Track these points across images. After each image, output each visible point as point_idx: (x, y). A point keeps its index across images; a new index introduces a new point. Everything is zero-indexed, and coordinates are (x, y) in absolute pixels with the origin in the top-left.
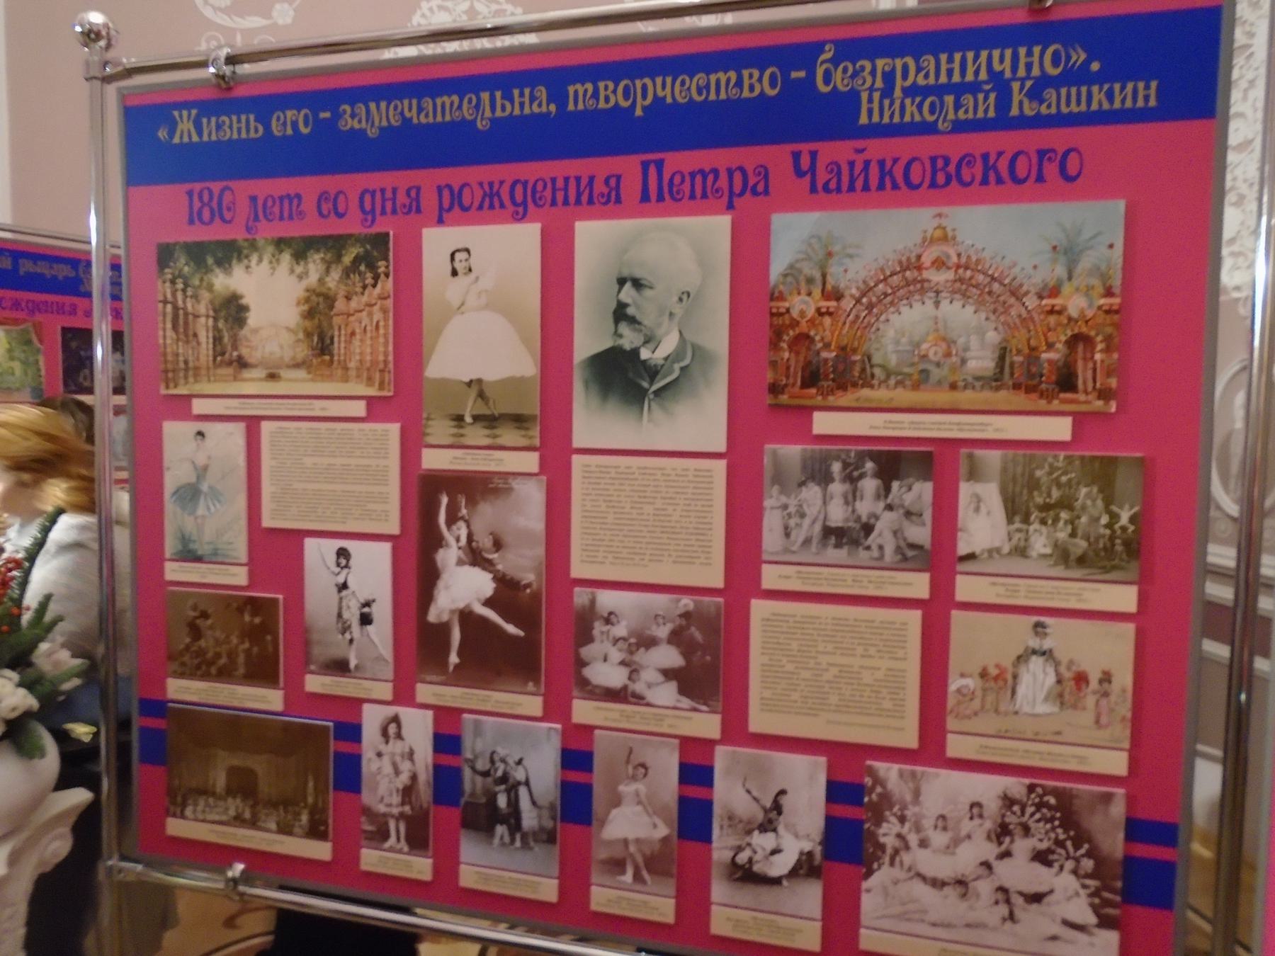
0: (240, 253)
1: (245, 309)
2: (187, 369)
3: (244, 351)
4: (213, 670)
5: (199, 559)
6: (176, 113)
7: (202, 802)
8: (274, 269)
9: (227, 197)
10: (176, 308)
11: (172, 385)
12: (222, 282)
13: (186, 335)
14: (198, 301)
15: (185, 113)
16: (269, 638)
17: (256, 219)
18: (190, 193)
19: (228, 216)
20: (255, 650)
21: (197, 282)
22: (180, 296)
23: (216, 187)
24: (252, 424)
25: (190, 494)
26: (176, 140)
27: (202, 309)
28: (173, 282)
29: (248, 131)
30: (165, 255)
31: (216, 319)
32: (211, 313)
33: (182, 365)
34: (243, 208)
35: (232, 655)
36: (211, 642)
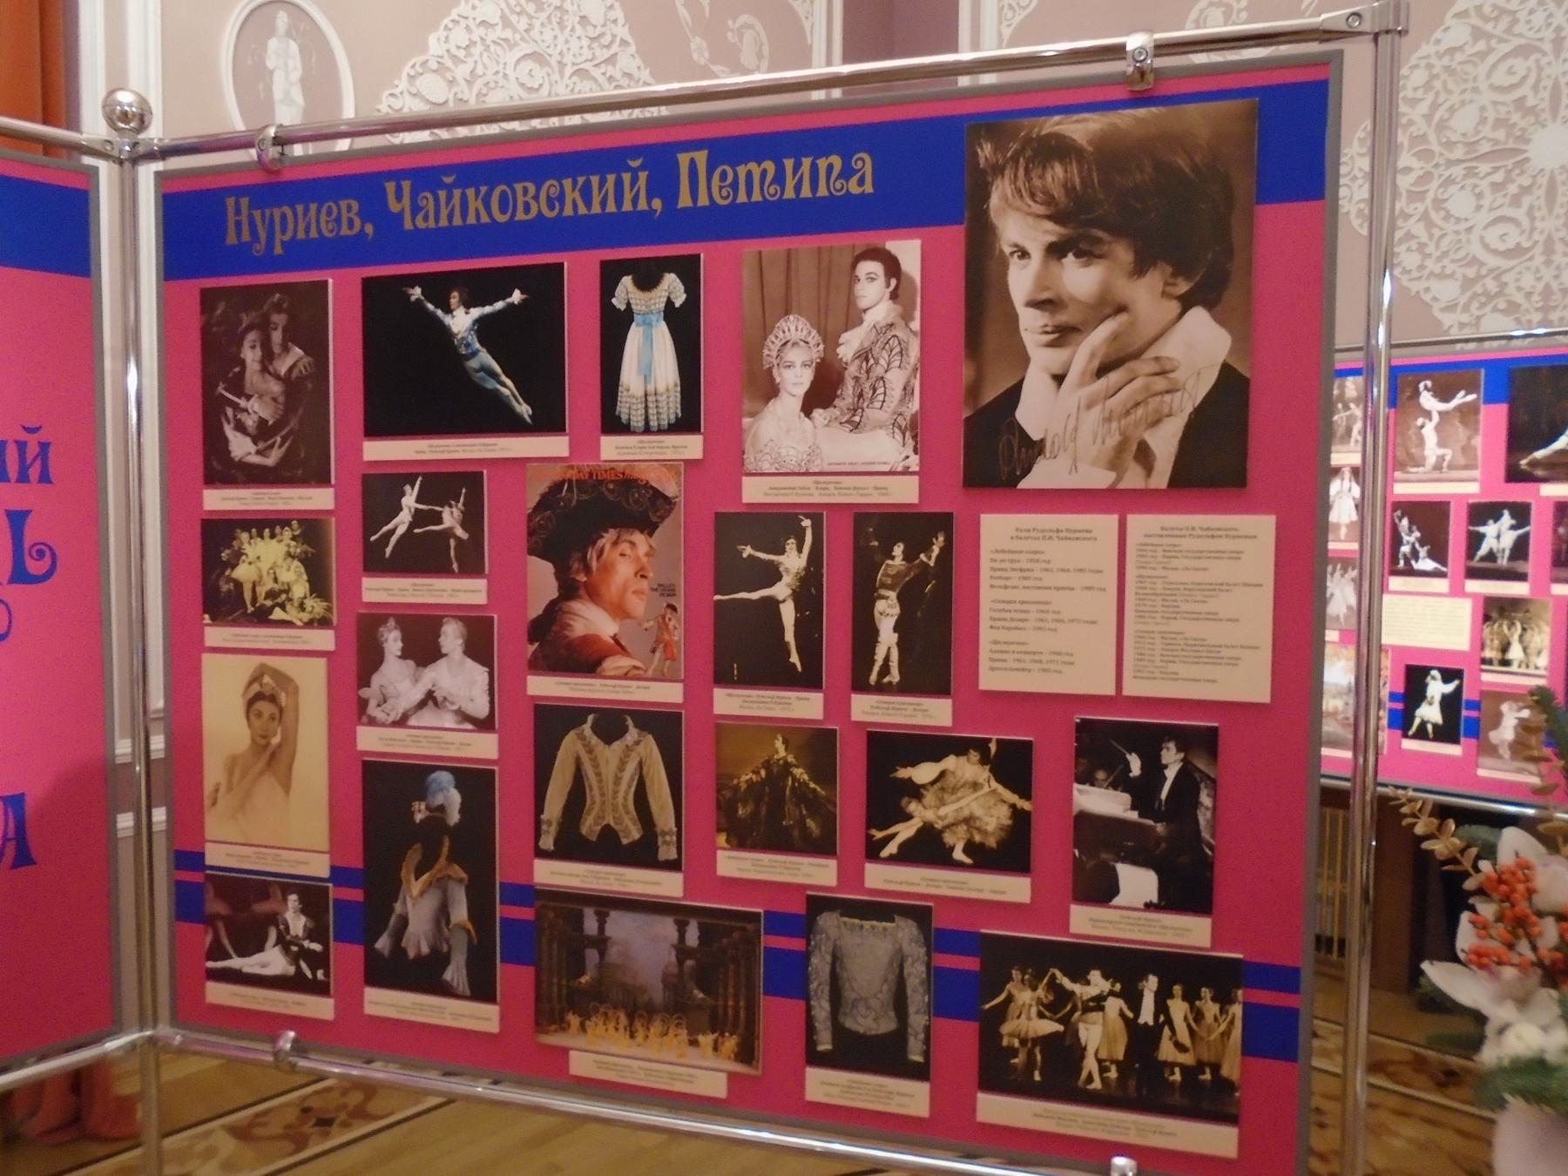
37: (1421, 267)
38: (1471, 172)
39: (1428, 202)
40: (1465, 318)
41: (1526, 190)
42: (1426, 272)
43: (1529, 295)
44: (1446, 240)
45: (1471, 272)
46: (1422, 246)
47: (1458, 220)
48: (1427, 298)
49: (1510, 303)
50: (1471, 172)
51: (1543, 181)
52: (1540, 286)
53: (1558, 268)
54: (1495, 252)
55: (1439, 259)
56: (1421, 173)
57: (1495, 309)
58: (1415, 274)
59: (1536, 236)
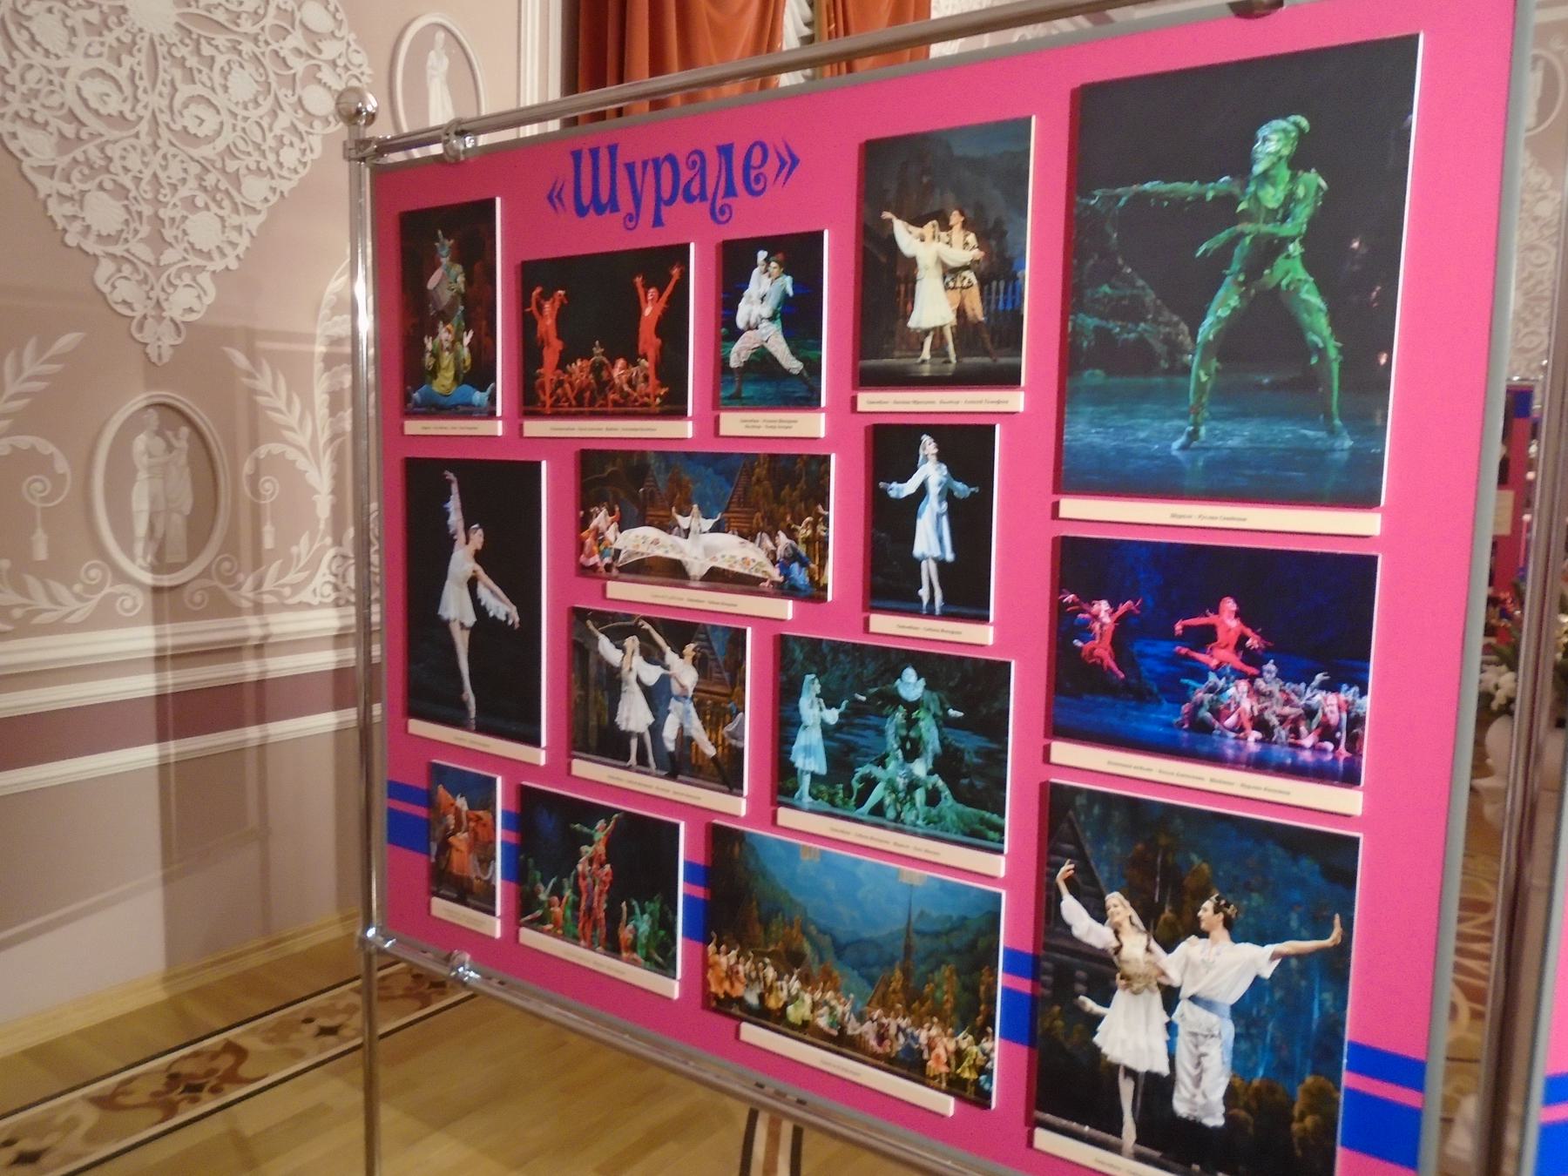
40: (66, 189)
44: (32, 76)
45: (69, 130)
47: (47, 53)
48: (13, 146)
51: (144, 44)
53: (165, 157)
54: (97, 113)
57: (101, 187)
59: (139, 107)
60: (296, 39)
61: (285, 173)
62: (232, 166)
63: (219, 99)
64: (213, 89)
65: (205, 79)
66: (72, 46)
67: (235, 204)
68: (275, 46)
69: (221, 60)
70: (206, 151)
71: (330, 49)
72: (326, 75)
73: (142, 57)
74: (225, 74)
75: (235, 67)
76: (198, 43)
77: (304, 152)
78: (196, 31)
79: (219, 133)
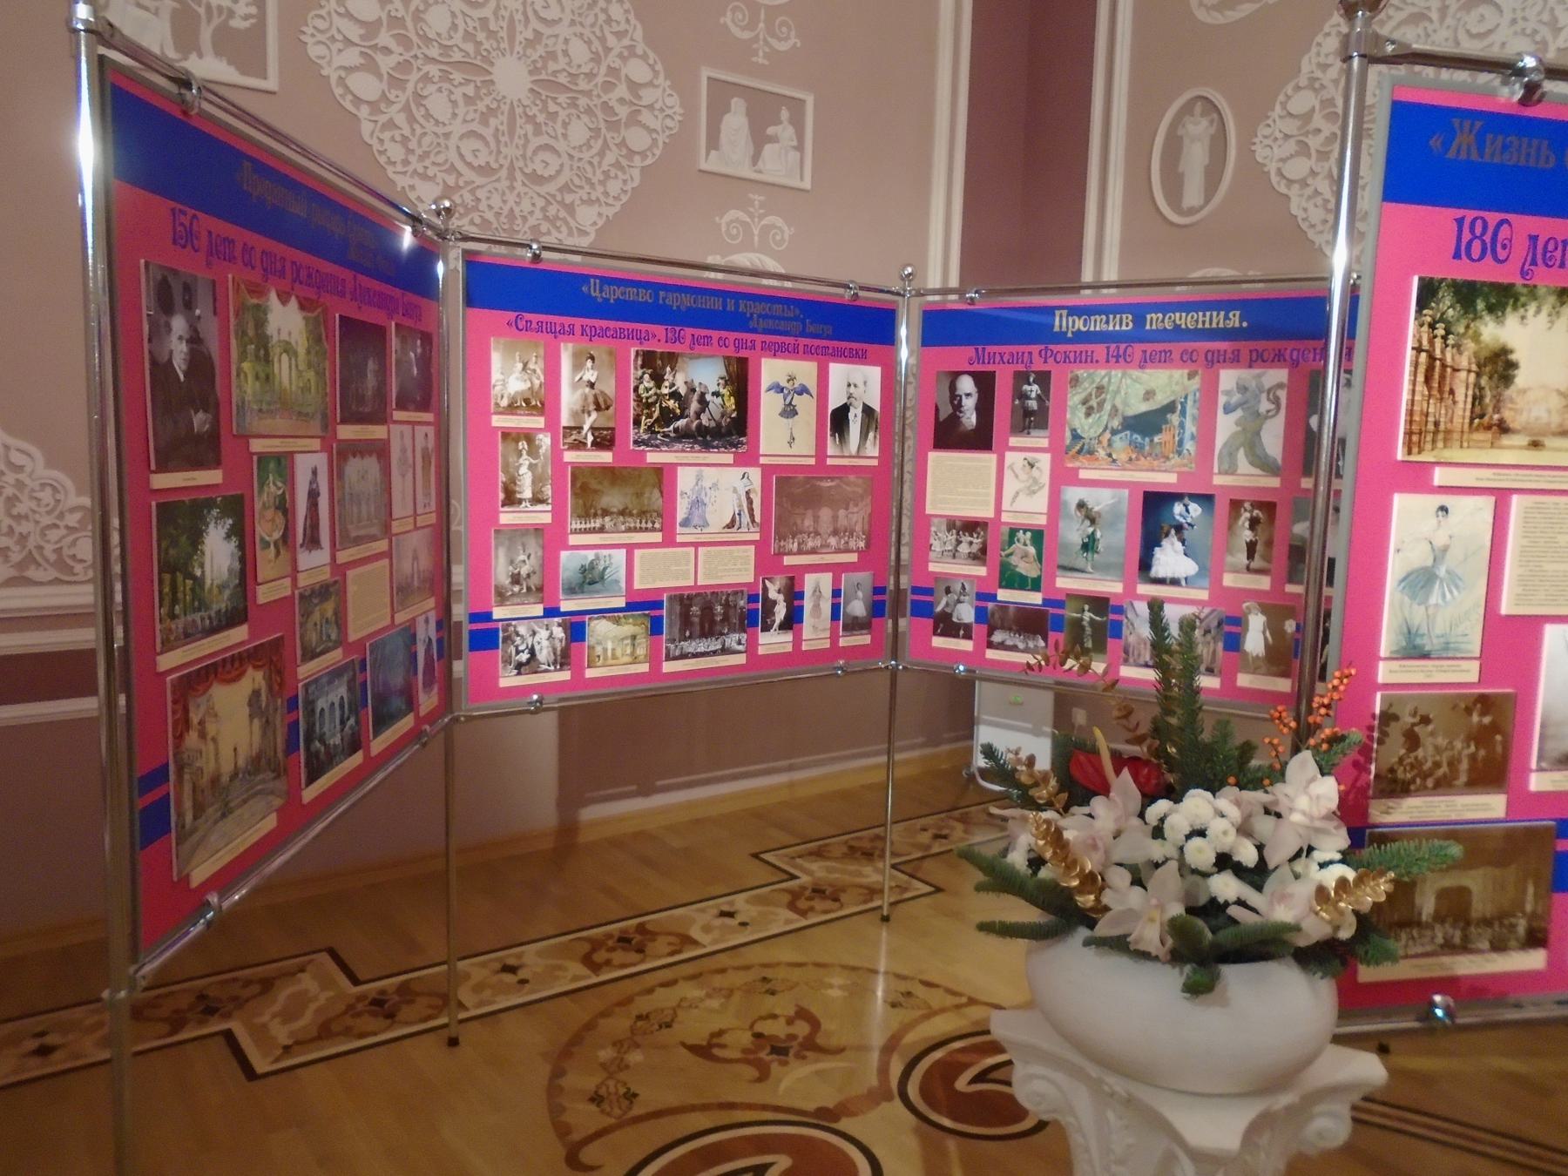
0: (1516, 300)
1: (1513, 365)
2: (1436, 432)
3: (1507, 414)
4: (1430, 783)
5: (1425, 656)
6: (1456, 122)
7: (1404, 936)
8: (1552, 322)
9: (1504, 232)
10: (1432, 358)
11: (1415, 450)
12: (1492, 331)
13: (1441, 391)
14: (1460, 353)
15: (1467, 124)
16: (1498, 738)
17: (1534, 263)
18: (1460, 222)
19: (1502, 254)
20: (1482, 753)
21: (1461, 330)
22: (1438, 343)
23: (1493, 218)
24: (1502, 497)
25: (1421, 581)
26: (1451, 154)
27: (1464, 362)
28: (1432, 326)
29: (1538, 159)
30: (1428, 292)
31: (1478, 375)
32: (1474, 367)
33: (1431, 427)
34: (1520, 249)
35: (1452, 764)
36: (1431, 750)
37: (406, 162)
38: (446, 76)
39: (409, 91)
41: (491, 112)
42: (410, 169)
43: (498, 214)
44: (427, 140)
45: (451, 180)
46: (405, 139)
47: (437, 122)
49: (484, 220)
50: (446, 76)
51: (506, 108)
52: (505, 212)
53: (519, 195)
54: (469, 164)
55: (421, 158)
56: (401, 59)
58: (399, 168)
60: (622, 91)
61: (610, 201)
62: (568, 198)
63: (561, 146)
64: (556, 138)
65: (550, 131)
66: (455, 115)
67: (570, 229)
68: (605, 98)
69: (563, 115)
70: (551, 188)
71: (648, 96)
72: (646, 117)
73: (505, 118)
74: (565, 125)
75: (574, 118)
76: (545, 103)
77: (625, 182)
78: (544, 93)
79: (559, 172)
